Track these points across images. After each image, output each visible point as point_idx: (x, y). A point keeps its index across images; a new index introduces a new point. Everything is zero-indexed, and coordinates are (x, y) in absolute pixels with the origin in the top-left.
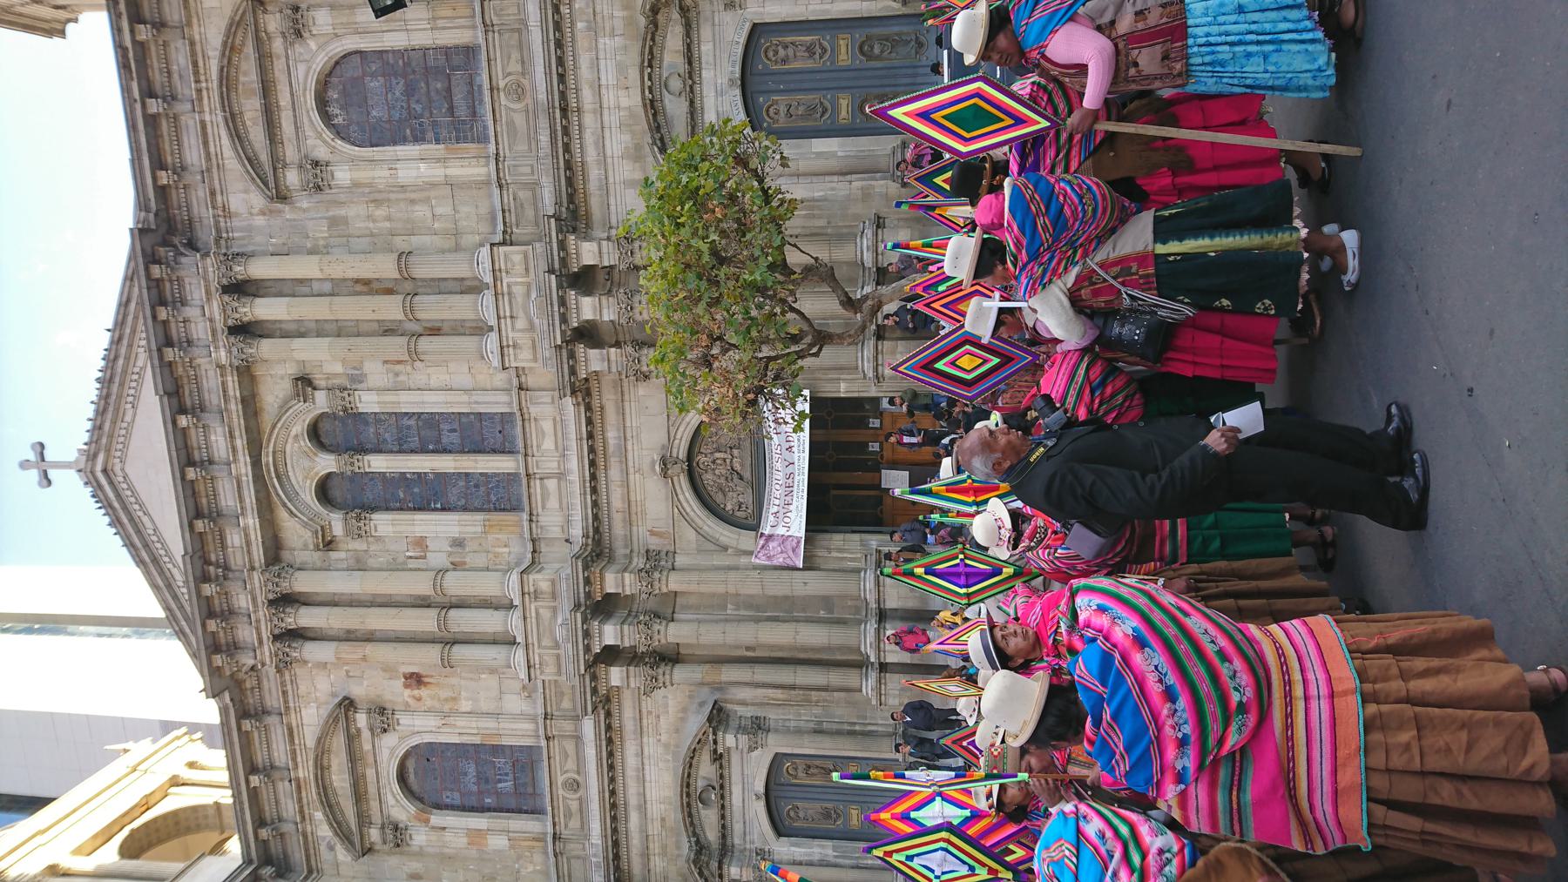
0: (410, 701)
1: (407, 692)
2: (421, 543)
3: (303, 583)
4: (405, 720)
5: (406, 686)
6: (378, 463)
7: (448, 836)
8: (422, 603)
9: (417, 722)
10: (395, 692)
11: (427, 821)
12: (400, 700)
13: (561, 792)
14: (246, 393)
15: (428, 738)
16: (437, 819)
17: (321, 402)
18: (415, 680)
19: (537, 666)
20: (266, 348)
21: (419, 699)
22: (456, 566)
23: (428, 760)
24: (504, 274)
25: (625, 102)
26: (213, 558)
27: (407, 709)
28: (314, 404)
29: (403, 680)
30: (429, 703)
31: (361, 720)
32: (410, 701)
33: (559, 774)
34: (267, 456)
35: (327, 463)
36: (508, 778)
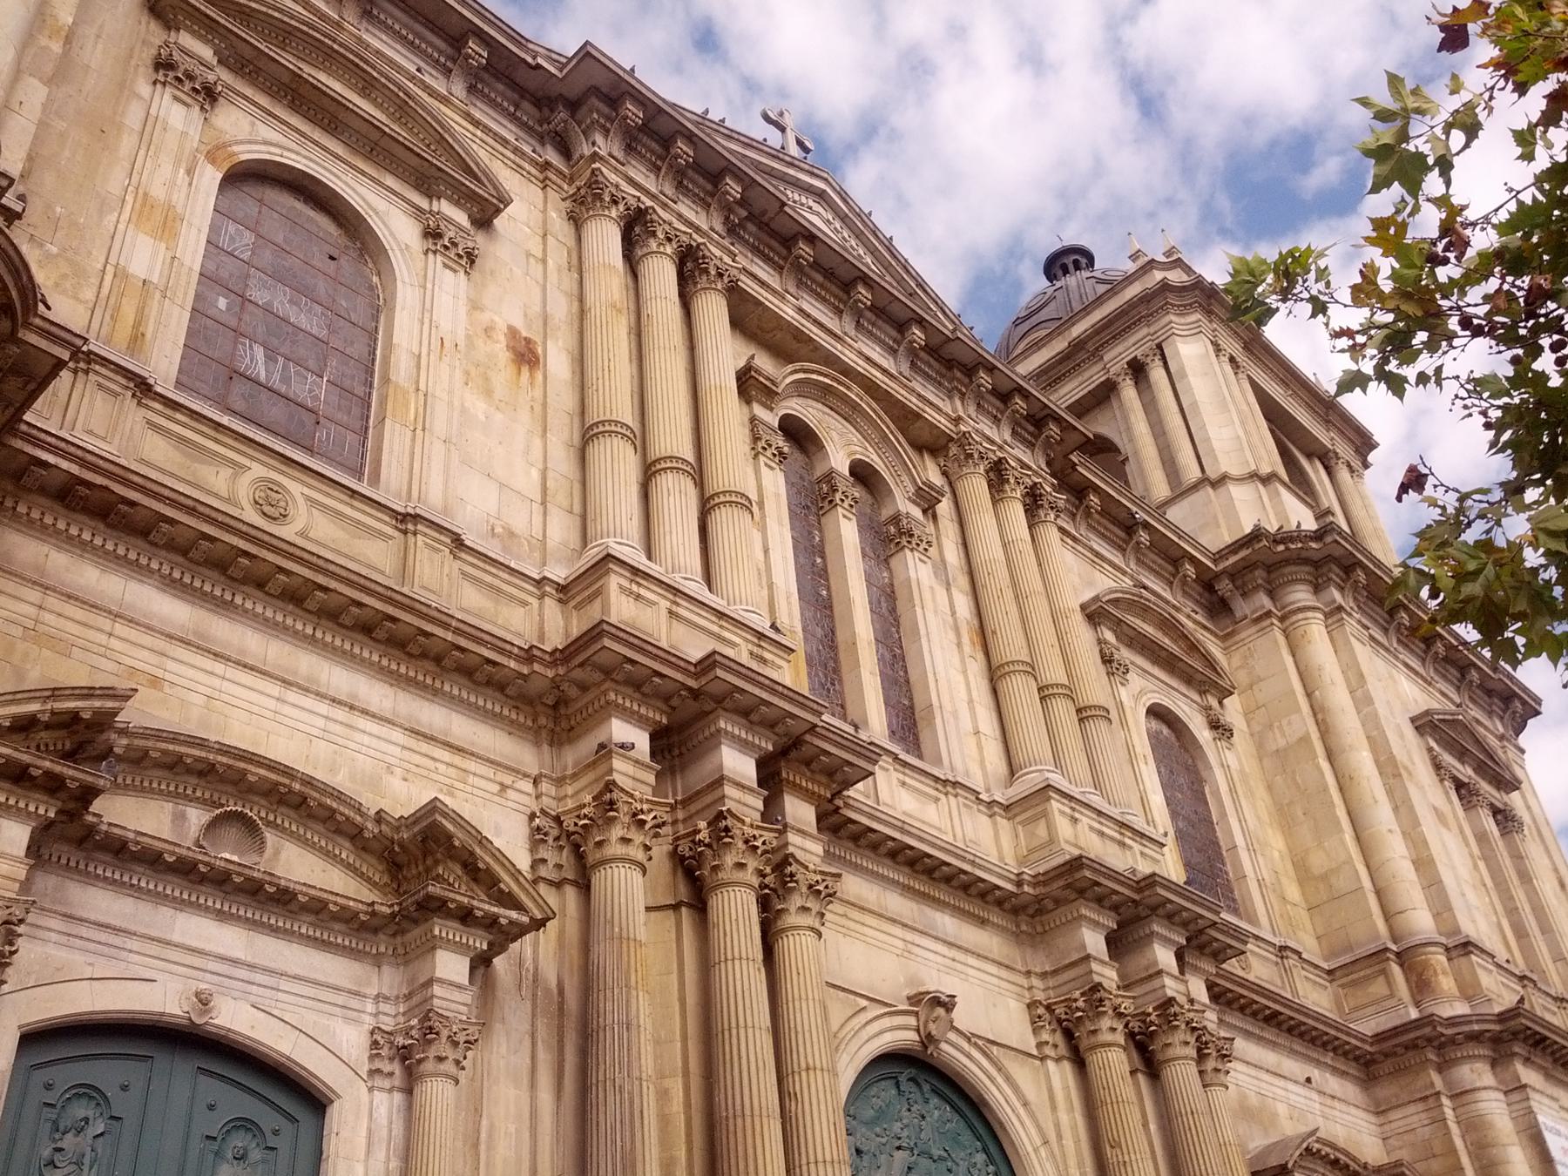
0: (485, 317)
1: (502, 326)
4: (450, 285)
13: (258, 470)
14: (918, 424)
15: (406, 296)
18: (526, 355)
19: (635, 588)
20: (976, 486)
23: (332, 258)
24: (1141, 848)
25: (1282, 1109)
26: (751, 227)
28: (909, 499)
29: (524, 334)
30: (479, 343)
33: (307, 491)
34: (857, 395)
35: (839, 461)
36: (277, 376)
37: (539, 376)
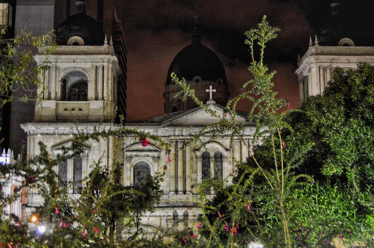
0: (160, 166)
1: (162, 166)
2: (196, 172)
3: (188, 149)
5: (164, 166)
6: (212, 165)
7: (129, 172)
8: (184, 172)
9: (156, 168)
10: (163, 163)
11: (132, 167)
12: (161, 164)
16: (132, 169)
17: (225, 154)
21: (161, 168)
22: (191, 179)
27: (158, 165)
31: (156, 154)
32: (160, 166)
35: (212, 154)
37: (167, 170)
